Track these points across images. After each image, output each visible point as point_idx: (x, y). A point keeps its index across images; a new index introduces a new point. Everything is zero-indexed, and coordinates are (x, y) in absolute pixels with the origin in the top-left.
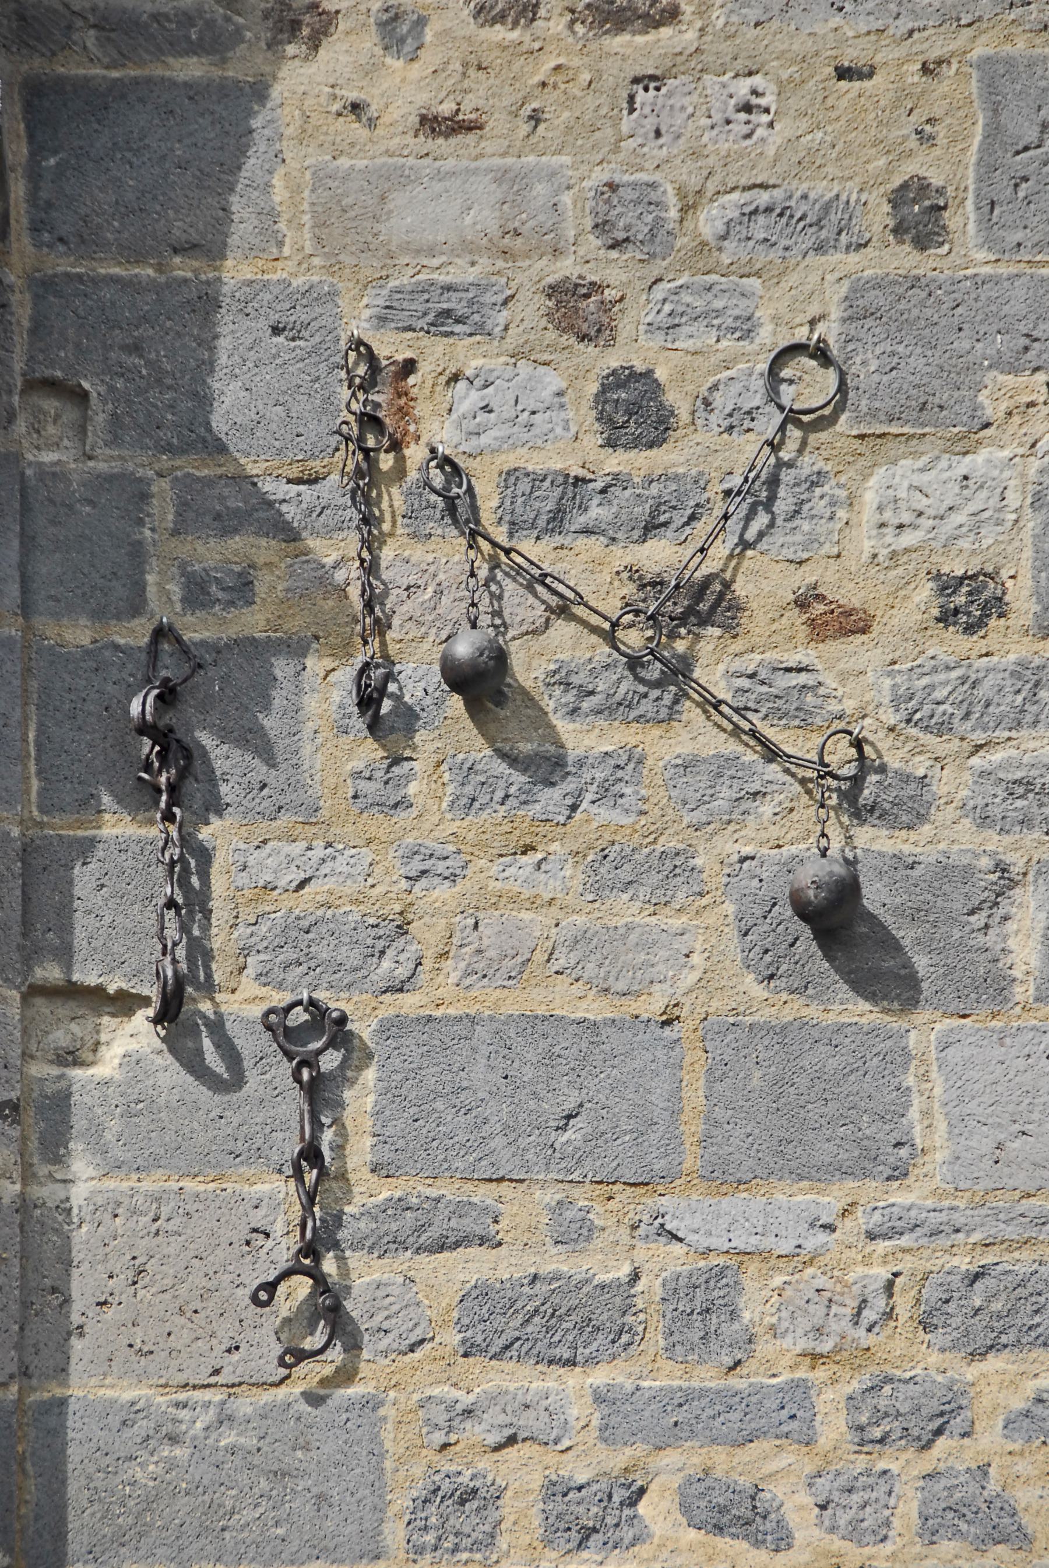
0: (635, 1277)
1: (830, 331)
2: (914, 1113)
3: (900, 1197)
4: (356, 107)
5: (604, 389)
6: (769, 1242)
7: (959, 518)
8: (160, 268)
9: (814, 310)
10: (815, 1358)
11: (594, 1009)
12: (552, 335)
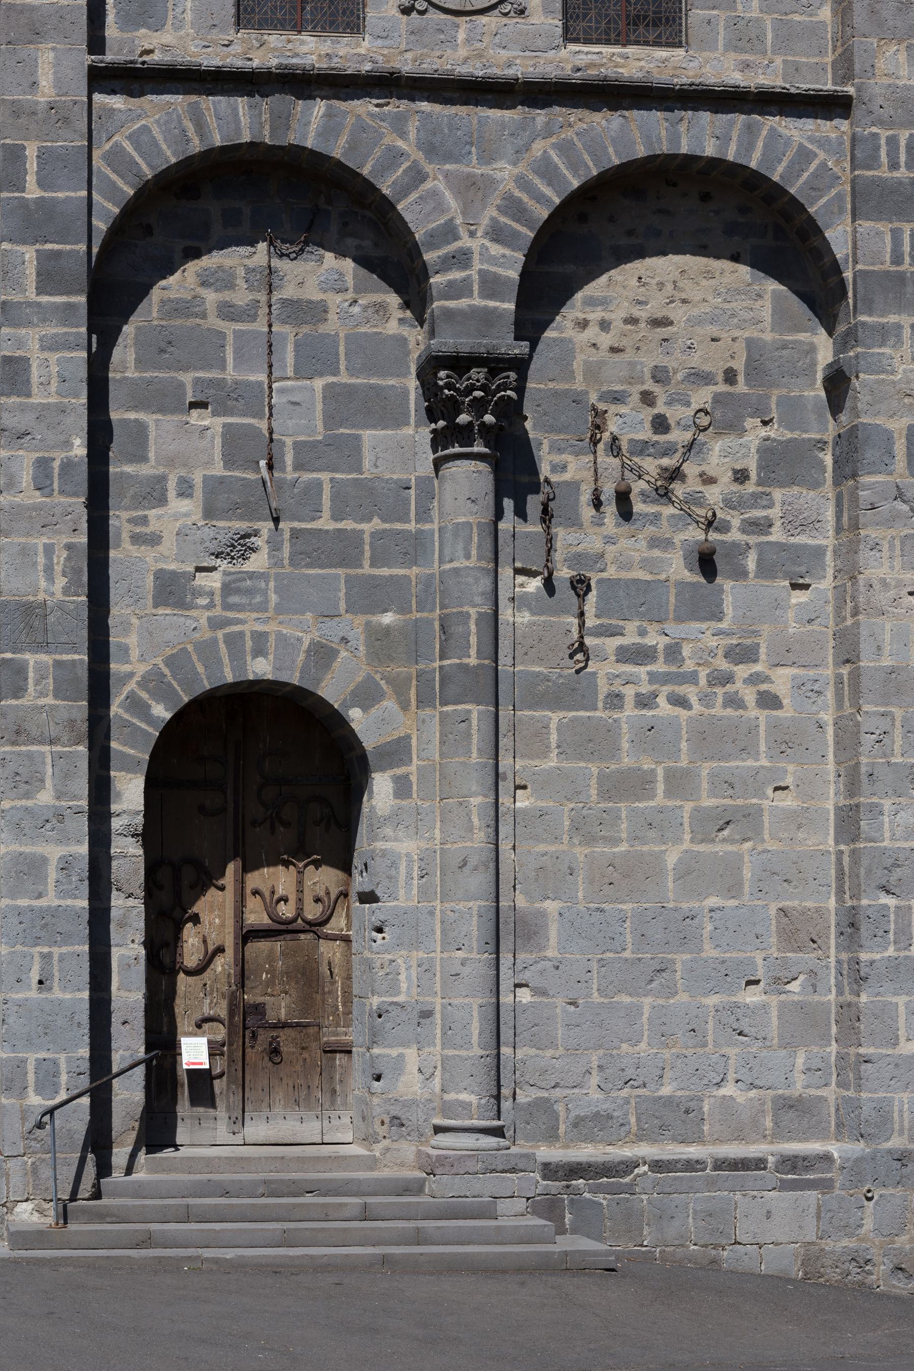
0: (657, 644)
1: (708, 407)
2: (724, 605)
3: (721, 626)
4: (594, 345)
5: (653, 419)
6: (688, 636)
7: (739, 455)
8: (546, 385)
9: (705, 400)
10: (699, 664)
11: (649, 577)
12: (641, 404)
